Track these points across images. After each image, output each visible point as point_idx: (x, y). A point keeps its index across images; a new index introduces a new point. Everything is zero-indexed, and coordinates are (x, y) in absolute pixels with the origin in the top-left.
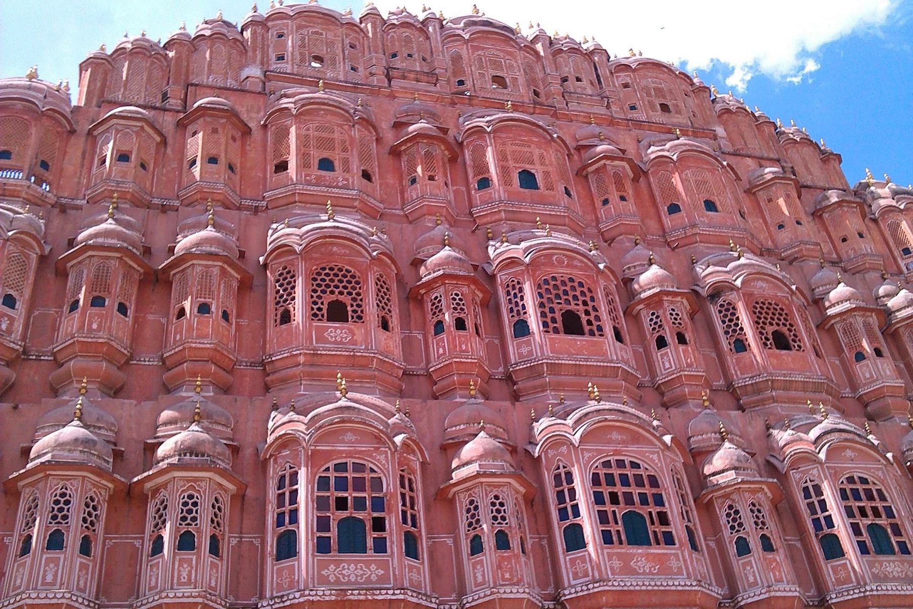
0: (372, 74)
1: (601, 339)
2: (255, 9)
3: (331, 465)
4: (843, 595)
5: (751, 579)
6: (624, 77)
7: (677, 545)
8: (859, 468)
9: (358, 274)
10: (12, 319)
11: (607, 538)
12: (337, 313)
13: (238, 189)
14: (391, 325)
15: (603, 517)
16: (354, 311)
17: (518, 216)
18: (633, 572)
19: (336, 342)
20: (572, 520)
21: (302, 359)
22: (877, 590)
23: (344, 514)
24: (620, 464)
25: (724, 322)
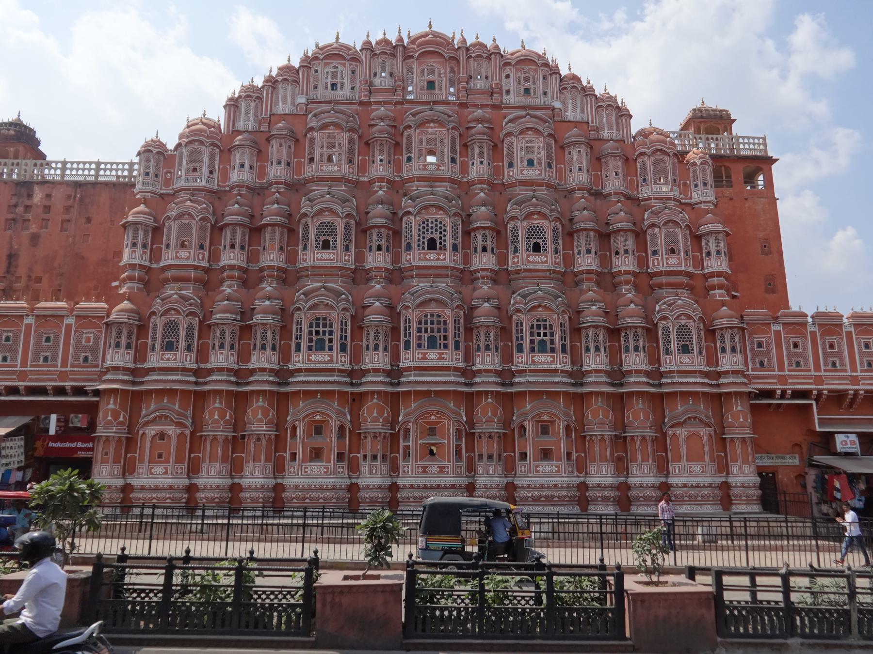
6: (508, 70)
10: (203, 254)
11: (419, 346)
12: (326, 245)
15: (419, 338)
23: (318, 337)
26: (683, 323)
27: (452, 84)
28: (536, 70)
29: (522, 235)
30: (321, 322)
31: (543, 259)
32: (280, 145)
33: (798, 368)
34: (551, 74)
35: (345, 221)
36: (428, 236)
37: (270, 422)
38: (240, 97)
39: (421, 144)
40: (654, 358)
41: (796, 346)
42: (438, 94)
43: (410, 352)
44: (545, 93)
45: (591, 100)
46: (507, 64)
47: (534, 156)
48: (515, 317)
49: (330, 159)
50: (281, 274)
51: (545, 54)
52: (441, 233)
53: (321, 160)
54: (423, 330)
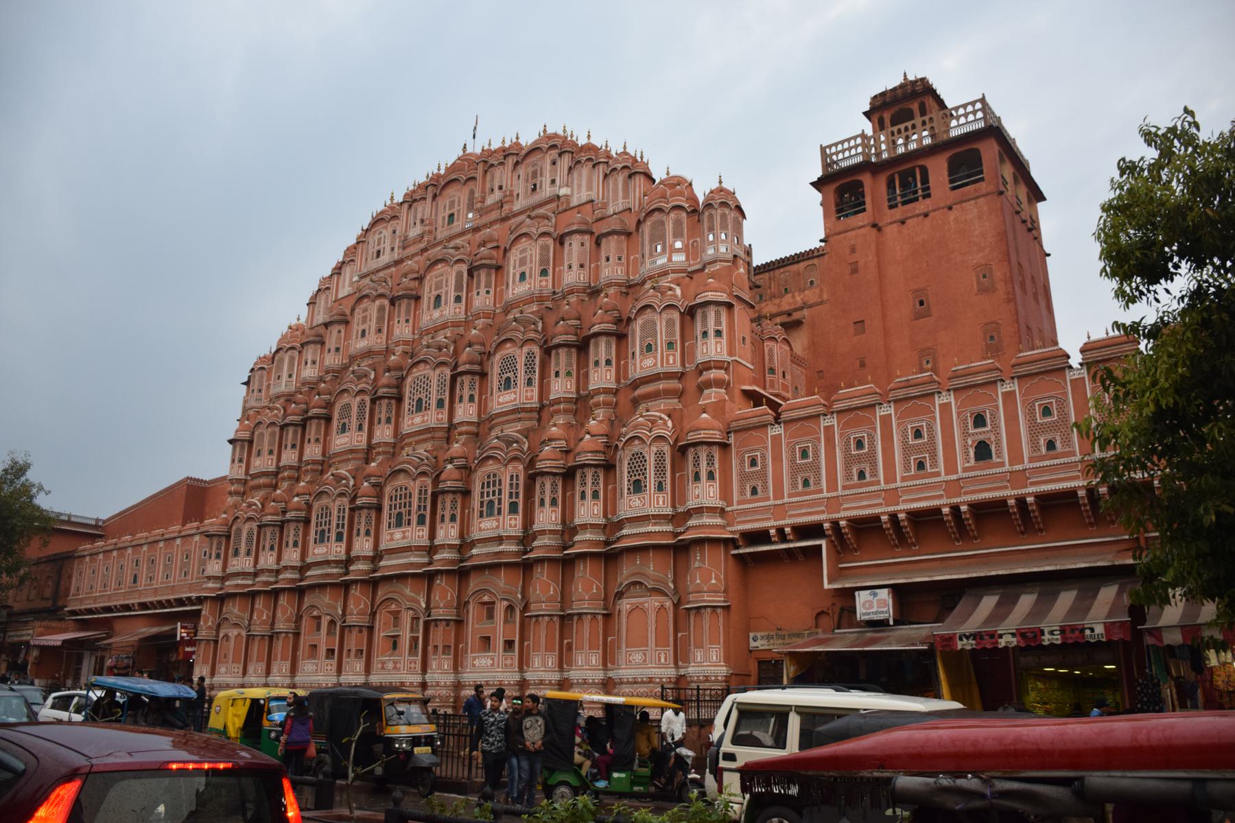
26: (636, 449)
28: (543, 158)
29: (496, 370)
31: (513, 396)
33: (807, 489)
34: (560, 155)
35: (358, 399)
36: (416, 398)
37: (288, 620)
40: (610, 506)
41: (804, 454)
44: (553, 181)
46: (517, 164)
47: (526, 269)
50: (315, 467)
51: (565, 131)
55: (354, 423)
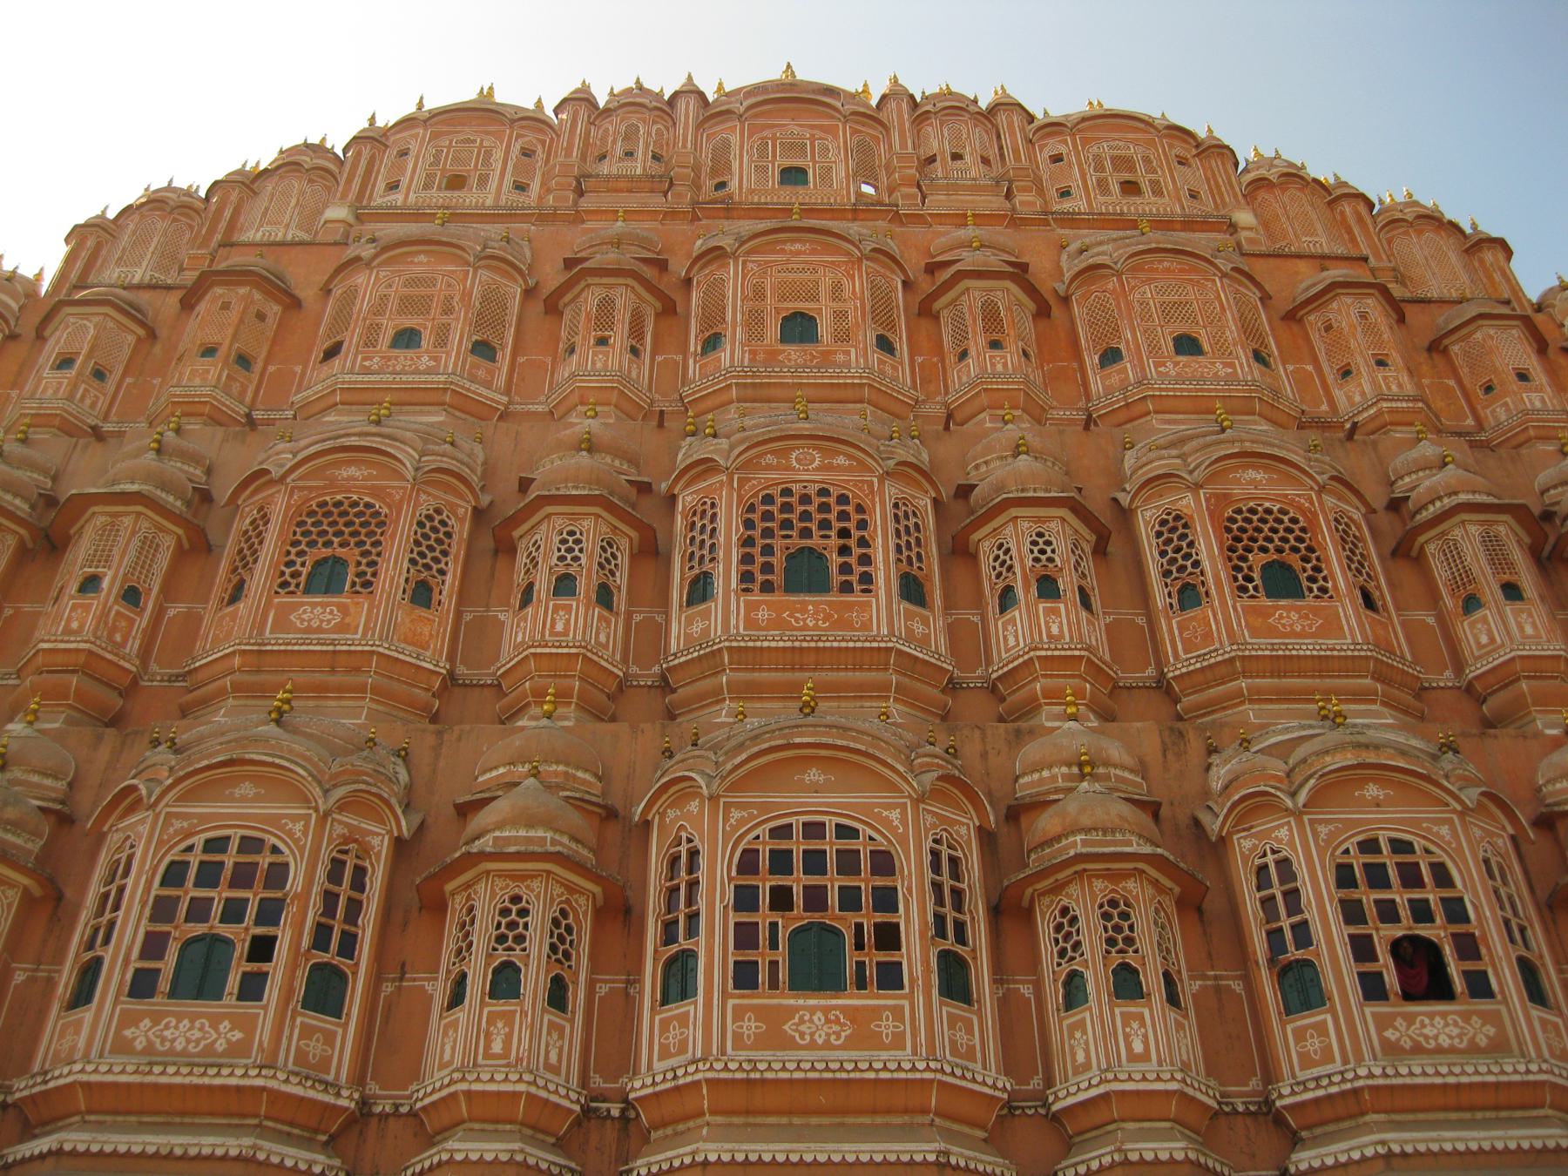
0: (549, 191)
1: (864, 598)
2: (372, 119)
3: (199, 840)
4: (1306, 1089)
5: (1081, 1057)
6: (1054, 146)
7: (907, 990)
8: (1387, 821)
9: (385, 510)
11: (745, 977)
12: (327, 578)
13: (249, 394)
14: (436, 597)
15: (745, 936)
16: (360, 574)
17: (765, 393)
18: (790, 1044)
19: (309, 630)
20: (683, 943)
21: (237, 661)
22: (1385, 1075)
24: (814, 830)
25: (1163, 554)
27: (866, 171)
30: (230, 859)
32: (226, 306)
38: (128, 210)
39: (759, 294)
42: (811, 193)
43: (693, 1008)
44: (1194, 195)
45: (1360, 220)
48: (1243, 844)
49: (407, 338)
52: (844, 533)
53: (370, 342)
54: (765, 899)
55: (394, 569)
